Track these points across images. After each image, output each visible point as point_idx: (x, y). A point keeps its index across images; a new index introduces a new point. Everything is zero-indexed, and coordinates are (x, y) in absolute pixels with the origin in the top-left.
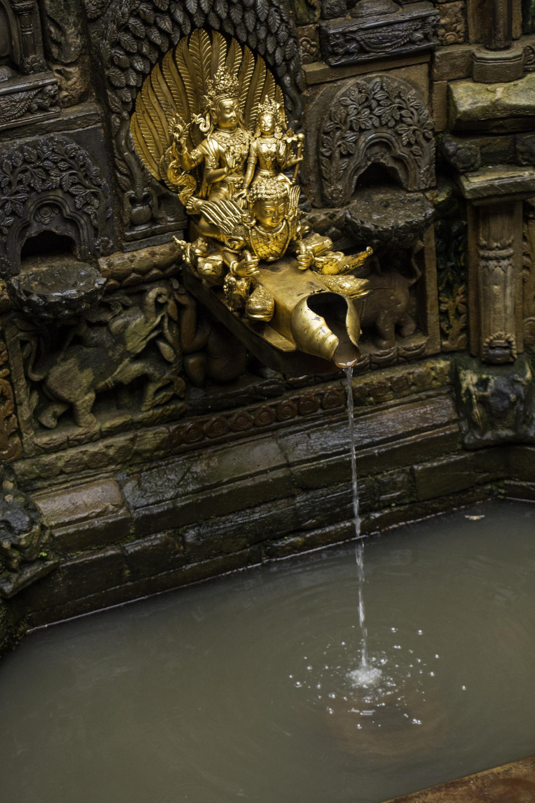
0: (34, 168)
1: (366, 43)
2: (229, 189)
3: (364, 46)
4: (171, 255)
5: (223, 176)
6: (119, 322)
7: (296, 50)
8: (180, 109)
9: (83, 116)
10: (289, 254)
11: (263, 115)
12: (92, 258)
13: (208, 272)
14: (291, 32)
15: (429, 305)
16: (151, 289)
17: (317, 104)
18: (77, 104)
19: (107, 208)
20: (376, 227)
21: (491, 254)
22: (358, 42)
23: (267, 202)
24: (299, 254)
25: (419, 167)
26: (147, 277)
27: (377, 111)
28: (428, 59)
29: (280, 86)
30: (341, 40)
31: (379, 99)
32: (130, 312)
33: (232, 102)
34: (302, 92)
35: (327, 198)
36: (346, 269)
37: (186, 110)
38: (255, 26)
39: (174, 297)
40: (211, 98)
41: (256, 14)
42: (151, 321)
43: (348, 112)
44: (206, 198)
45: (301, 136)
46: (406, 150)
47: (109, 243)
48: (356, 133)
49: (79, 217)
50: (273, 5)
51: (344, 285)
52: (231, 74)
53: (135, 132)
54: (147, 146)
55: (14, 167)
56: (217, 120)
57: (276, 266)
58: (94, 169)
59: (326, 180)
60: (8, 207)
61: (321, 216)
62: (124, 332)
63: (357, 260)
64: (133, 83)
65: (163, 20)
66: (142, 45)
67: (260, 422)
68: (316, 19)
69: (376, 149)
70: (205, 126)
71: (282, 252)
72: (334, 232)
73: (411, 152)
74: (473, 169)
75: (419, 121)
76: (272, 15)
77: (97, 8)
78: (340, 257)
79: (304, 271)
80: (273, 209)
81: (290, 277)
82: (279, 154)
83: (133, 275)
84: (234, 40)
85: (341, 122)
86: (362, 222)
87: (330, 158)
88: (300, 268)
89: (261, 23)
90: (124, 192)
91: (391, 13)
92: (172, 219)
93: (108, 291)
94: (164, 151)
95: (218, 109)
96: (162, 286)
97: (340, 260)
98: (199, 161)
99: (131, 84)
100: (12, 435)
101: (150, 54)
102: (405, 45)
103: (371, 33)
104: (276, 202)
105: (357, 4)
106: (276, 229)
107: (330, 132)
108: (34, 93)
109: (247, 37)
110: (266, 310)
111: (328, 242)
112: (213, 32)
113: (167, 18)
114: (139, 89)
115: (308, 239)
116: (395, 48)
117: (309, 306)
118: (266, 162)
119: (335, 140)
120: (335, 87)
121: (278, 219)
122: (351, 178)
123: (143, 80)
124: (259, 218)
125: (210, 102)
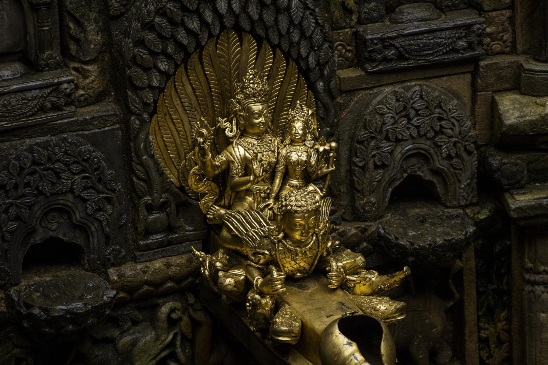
0: (44, 170)
1: (405, 50)
2: (254, 199)
3: (404, 53)
4: (187, 267)
5: (249, 185)
6: (127, 339)
7: (330, 54)
8: (205, 112)
9: (100, 117)
10: (319, 271)
11: (294, 121)
12: (101, 268)
13: (229, 287)
14: (326, 37)
15: (467, 331)
16: (164, 303)
17: (351, 111)
18: (94, 104)
19: (121, 215)
20: (412, 244)
21: (538, 278)
22: (397, 48)
23: (297, 215)
24: (330, 271)
25: (459, 181)
26: (161, 290)
27: (415, 121)
28: (471, 69)
29: (313, 92)
30: (379, 46)
31: (418, 108)
32: (140, 327)
33: (261, 107)
34: (336, 98)
35: (359, 210)
36: (381, 290)
37: (211, 113)
38: (289, 29)
39: (189, 313)
40: (239, 102)
41: (291, 17)
42: (163, 338)
43: (384, 121)
44: (229, 207)
45: (334, 144)
46: (445, 163)
47: (120, 252)
48: (392, 144)
49: (89, 224)
50: (309, 8)
51: (378, 307)
52: (261, 78)
53: (155, 134)
54: (168, 150)
55: (22, 169)
56: (245, 126)
57: (304, 284)
58: (109, 173)
59: (358, 191)
60: (13, 211)
61: (352, 229)
62: (132, 350)
63: (393, 280)
64: (155, 83)
65: (191, 19)
66: (167, 45)
68: (353, 23)
69: (414, 161)
70: (231, 131)
71: (311, 268)
72: (365, 247)
73: (451, 165)
74: (519, 186)
75: (460, 133)
76: (307, 18)
77: (121, 5)
78: (374, 277)
79: (335, 290)
80: (303, 223)
81: (319, 296)
82: (310, 163)
83: (146, 288)
84: (265, 42)
85: (376, 131)
86: (397, 239)
87: (363, 168)
88: (330, 286)
89: (295, 26)
90: (140, 197)
91: (432, 20)
92: (191, 229)
93: (117, 304)
94: (186, 156)
95: (246, 114)
96: (176, 301)
97: (373, 279)
98: (223, 167)
99: (154, 84)
101: (175, 54)
102: (447, 53)
103: (411, 40)
104: (306, 215)
105: (397, 10)
106: (306, 243)
107: (364, 141)
109: (280, 40)
110: (293, 332)
111: (360, 259)
112: (243, 33)
113: (195, 17)
114: (161, 90)
115: (339, 255)
116: (437, 56)
117: (340, 330)
118: (295, 170)
119: (369, 150)
120: (370, 94)
121: (308, 233)
122: (385, 191)
123: (167, 81)
124: (287, 231)
125: (238, 106)
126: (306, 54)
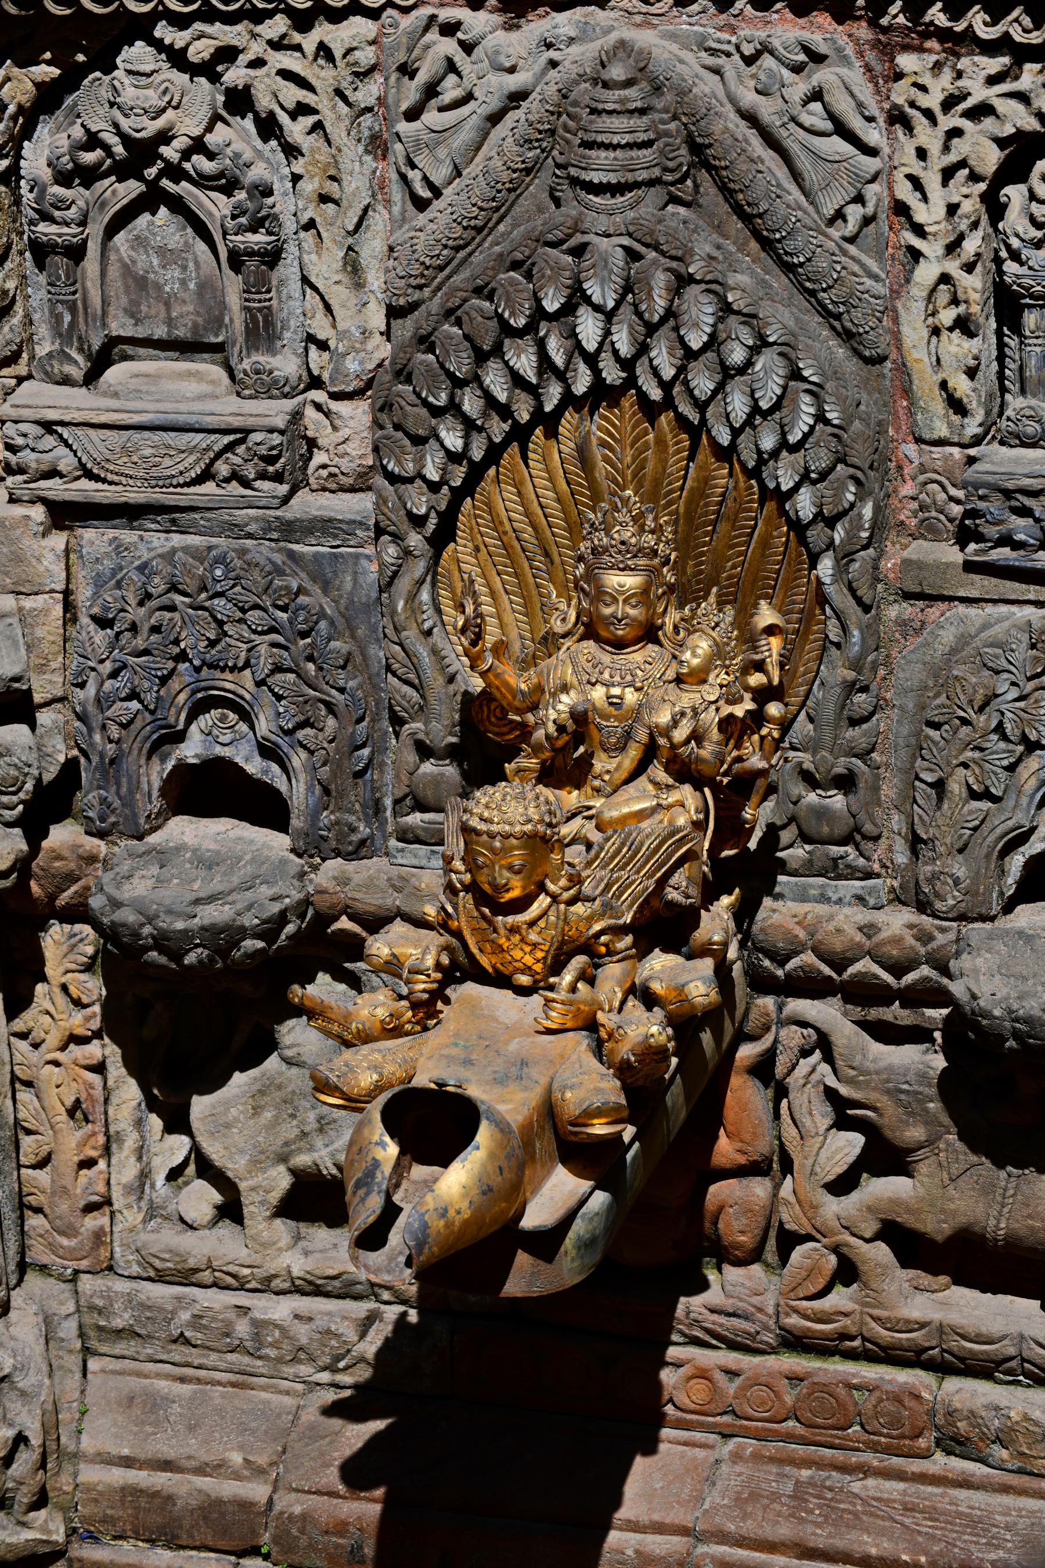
0: (191, 607)
20: (974, 997)
24: (551, 988)
38: (751, 417)
48: (1011, 747)
50: (805, 380)
55: (148, 596)
59: (925, 842)
64: (433, 475)
67: (687, 1401)
70: (564, 620)
72: (926, 979)
100: (90, 1208)
108: (227, 439)
126: (791, 484)
